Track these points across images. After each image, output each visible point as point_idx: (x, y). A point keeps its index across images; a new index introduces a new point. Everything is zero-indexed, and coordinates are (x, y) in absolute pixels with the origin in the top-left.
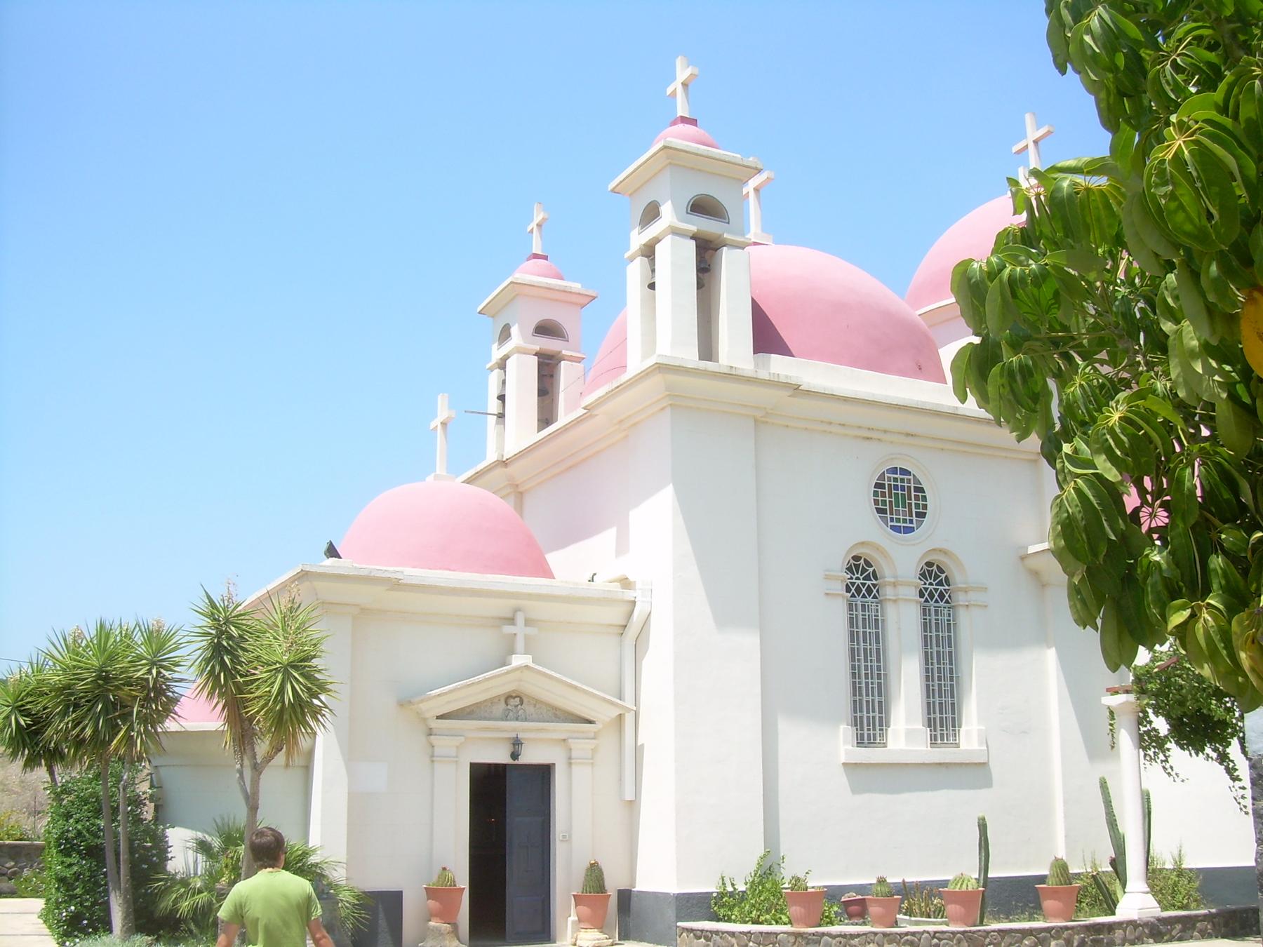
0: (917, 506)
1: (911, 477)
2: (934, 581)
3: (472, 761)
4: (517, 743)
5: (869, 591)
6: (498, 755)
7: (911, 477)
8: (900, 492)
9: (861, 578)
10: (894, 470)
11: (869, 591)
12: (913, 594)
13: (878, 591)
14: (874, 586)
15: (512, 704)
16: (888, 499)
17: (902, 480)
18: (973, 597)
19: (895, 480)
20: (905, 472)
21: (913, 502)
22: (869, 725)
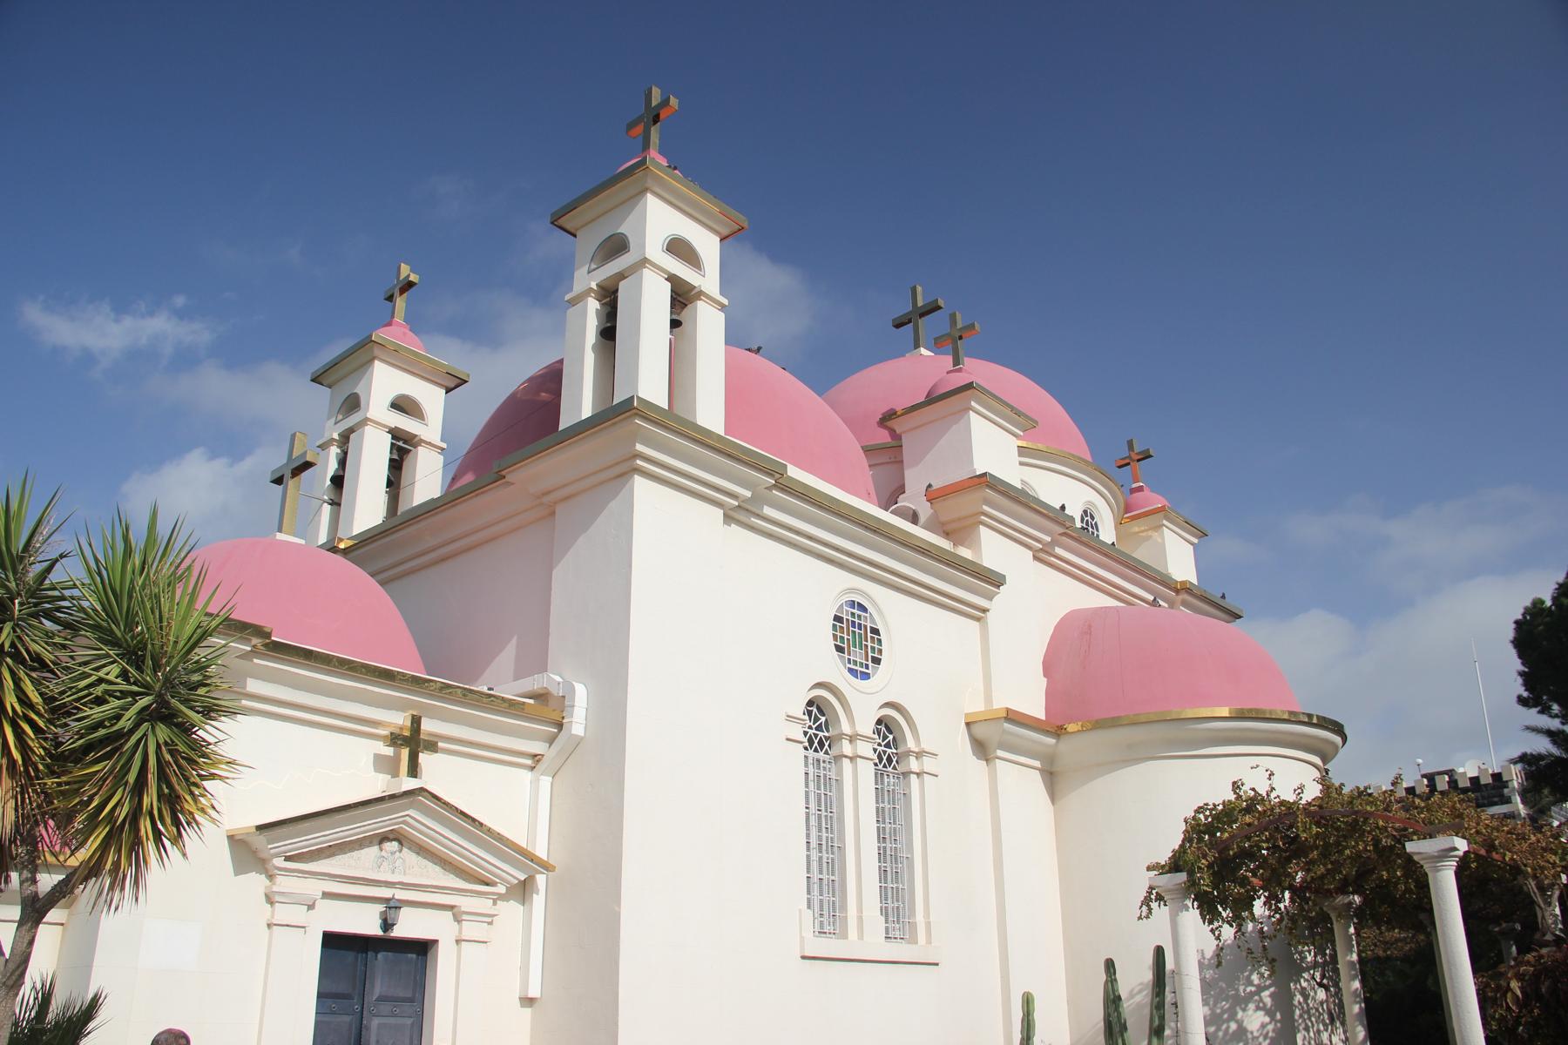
0: (873, 648)
1: (868, 615)
2: (883, 741)
3: (326, 930)
4: (392, 908)
5: (821, 744)
6: (365, 922)
7: (868, 615)
8: (856, 630)
9: (814, 727)
10: (852, 604)
11: (821, 744)
12: (866, 749)
13: (829, 746)
14: (827, 738)
15: (387, 849)
16: (846, 637)
17: (859, 616)
18: (928, 764)
19: (853, 614)
20: (863, 608)
21: (869, 644)
22: (822, 910)
